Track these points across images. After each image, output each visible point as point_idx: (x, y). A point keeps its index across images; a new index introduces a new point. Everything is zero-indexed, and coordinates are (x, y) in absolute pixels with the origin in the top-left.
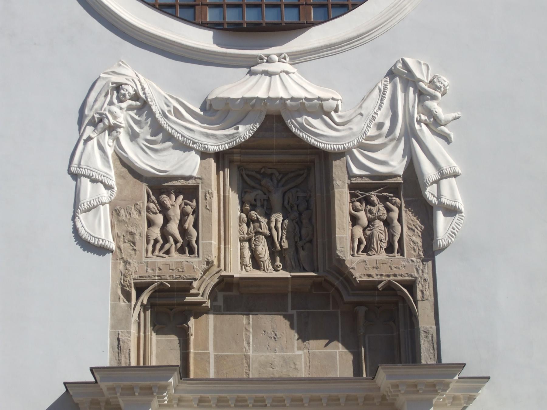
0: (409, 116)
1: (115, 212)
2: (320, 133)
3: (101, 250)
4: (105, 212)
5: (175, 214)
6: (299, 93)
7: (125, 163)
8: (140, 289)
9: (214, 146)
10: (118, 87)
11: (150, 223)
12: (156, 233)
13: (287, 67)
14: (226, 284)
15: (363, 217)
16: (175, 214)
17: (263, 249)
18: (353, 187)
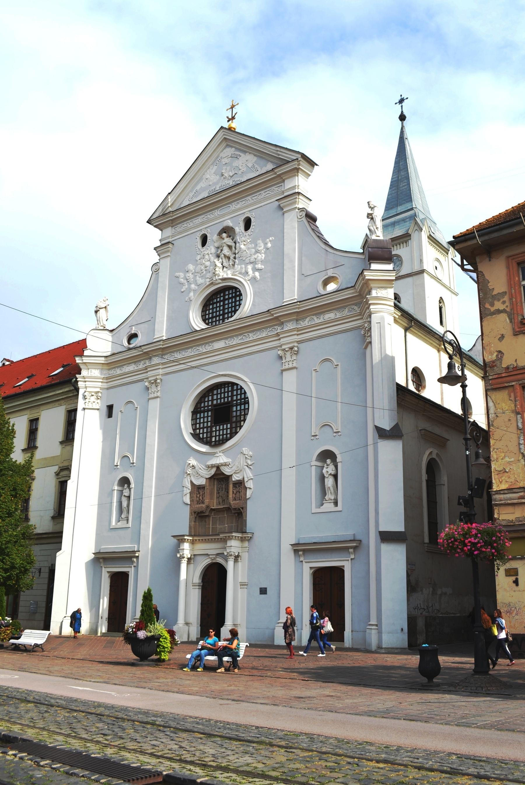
0: (243, 464)
1: (190, 495)
2: (227, 471)
3: (187, 504)
4: (188, 495)
5: (201, 493)
6: (222, 461)
7: (191, 482)
8: (195, 512)
9: (207, 477)
10: (190, 464)
11: (197, 497)
12: (198, 499)
13: (221, 454)
14: (214, 510)
15: (235, 492)
16: (201, 493)
17: (221, 500)
18: (233, 484)
